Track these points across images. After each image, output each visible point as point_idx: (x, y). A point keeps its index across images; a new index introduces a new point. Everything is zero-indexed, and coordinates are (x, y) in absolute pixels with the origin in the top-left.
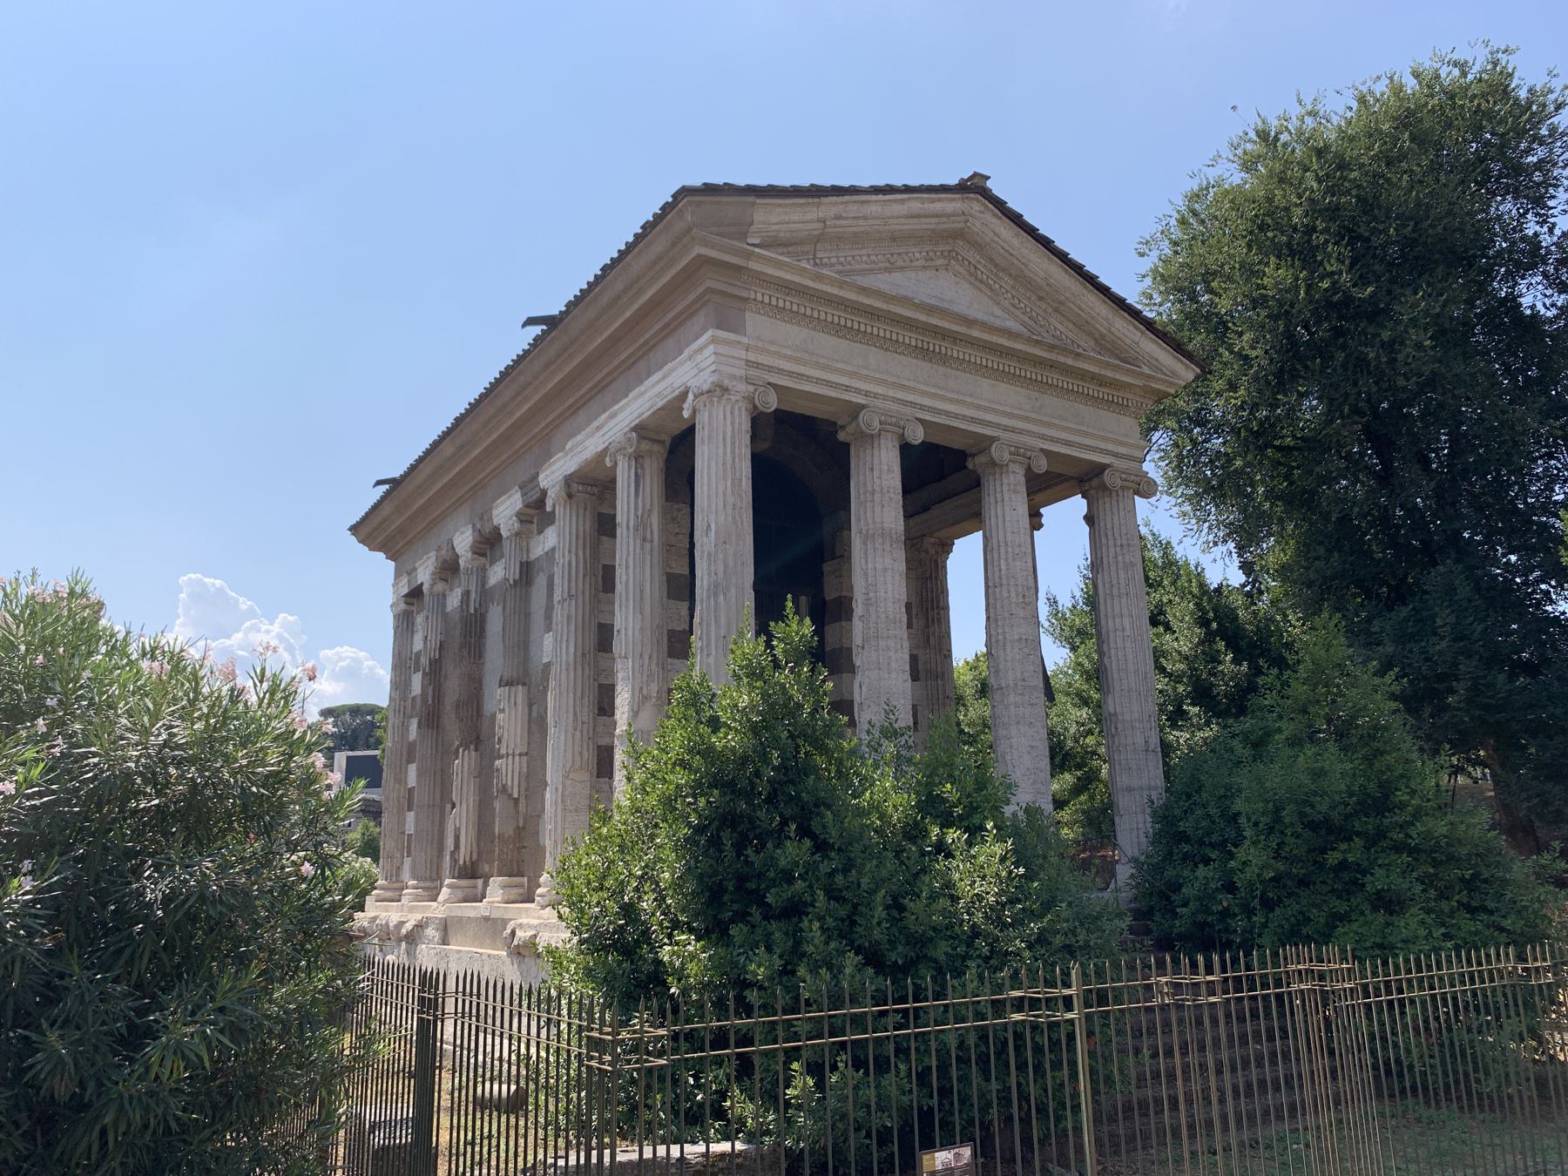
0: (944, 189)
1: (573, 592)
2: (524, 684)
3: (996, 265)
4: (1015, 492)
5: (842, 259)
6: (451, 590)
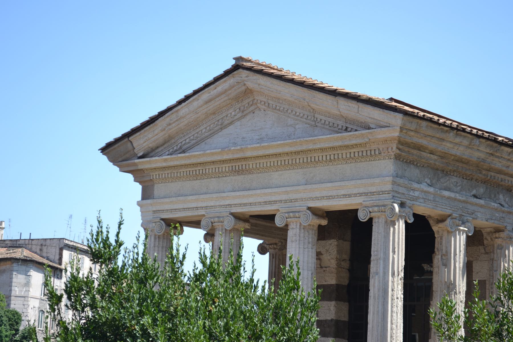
5: (192, 138)
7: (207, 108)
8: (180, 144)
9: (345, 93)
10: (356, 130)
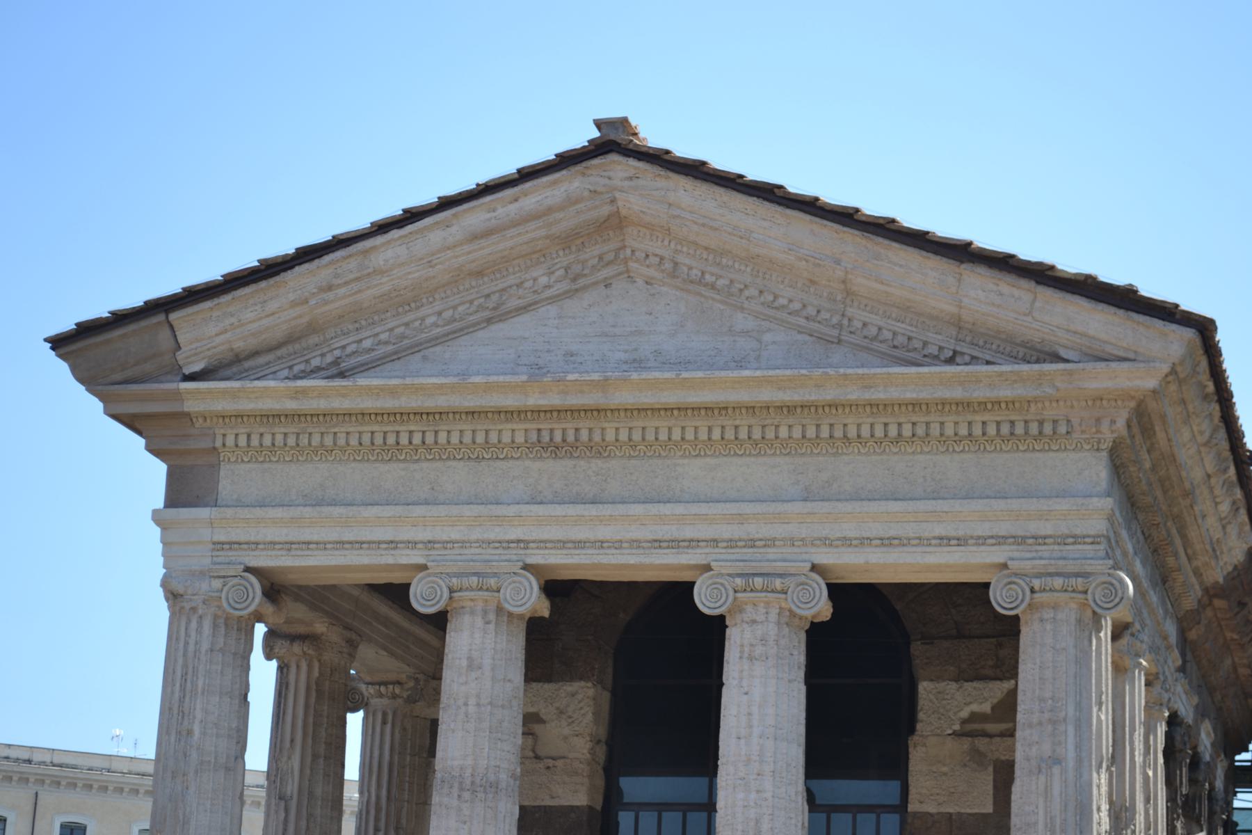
5: (384, 337)
7: (469, 253)
8: (337, 353)
9: (1001, 256)
10: (988, 363)
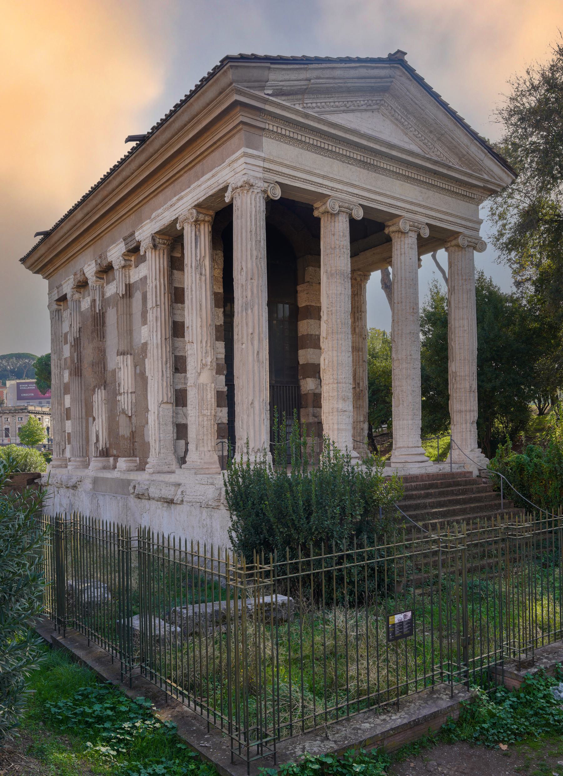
0: (380, 60)
1: (159, 303)
2: (131, 354)
3: (407, 110)
4: (411, 248)
5: (319, 104)
6: (84, 298)
